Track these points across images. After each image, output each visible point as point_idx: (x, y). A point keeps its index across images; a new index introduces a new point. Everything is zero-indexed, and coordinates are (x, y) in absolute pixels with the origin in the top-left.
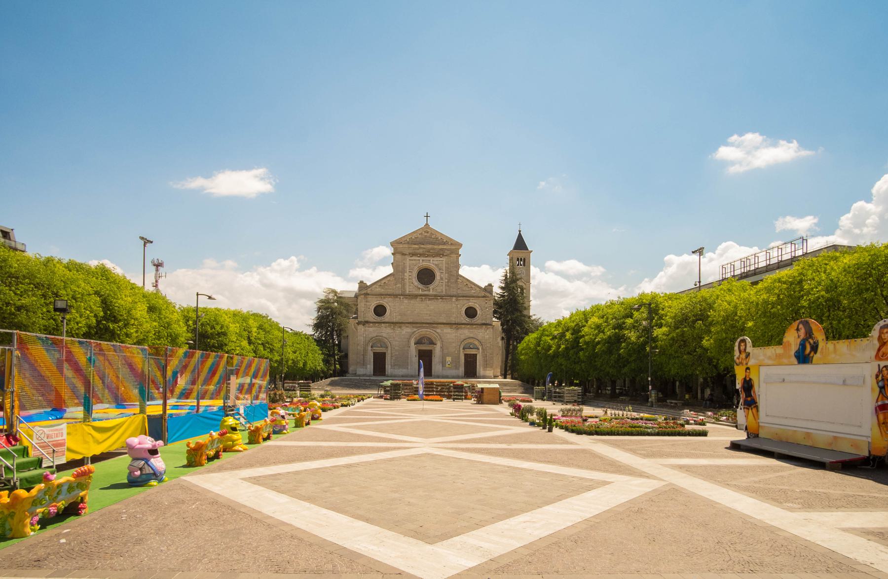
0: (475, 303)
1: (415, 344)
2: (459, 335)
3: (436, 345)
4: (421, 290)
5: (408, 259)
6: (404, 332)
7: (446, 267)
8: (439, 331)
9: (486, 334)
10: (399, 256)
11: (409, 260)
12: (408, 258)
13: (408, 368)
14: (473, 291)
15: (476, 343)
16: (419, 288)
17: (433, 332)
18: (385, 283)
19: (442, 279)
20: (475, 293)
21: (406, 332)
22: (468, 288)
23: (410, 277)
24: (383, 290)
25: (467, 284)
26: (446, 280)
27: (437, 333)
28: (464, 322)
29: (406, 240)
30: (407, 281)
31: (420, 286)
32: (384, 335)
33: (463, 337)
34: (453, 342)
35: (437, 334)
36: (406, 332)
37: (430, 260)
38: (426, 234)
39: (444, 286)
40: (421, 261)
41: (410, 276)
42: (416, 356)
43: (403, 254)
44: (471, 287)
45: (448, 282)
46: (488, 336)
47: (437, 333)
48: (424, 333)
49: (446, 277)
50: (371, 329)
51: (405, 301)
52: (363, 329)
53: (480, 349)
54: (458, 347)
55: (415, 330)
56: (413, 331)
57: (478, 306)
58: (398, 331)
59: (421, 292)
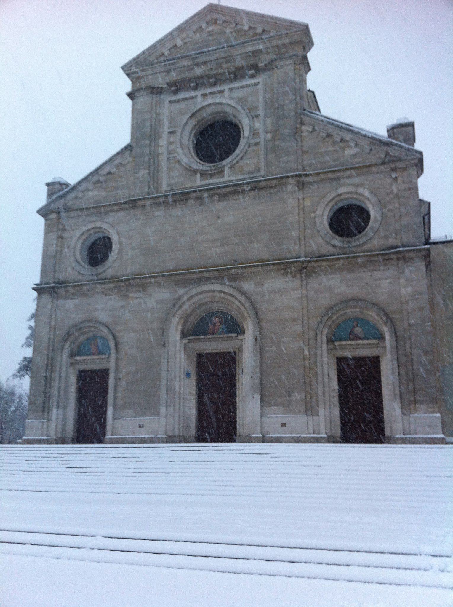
0: (357, 186)
1: (184, 335)
2: (312, 294)
3: (243, 333)
4: (198, 175)
5: (167, 102)
6: (151, 303)
7: (265, 100)
8: (248, 286)
9: (402, 281)
10: (144, 99)
11: (171, 102)
12: (167, 98)
13: (158, 414)
14: (349, 152)
15: (372, 315)
16: (195, 172)
17: (231, 291)
18: (109, 173)
19: (254, 133)
20: (354, 156)
21: (158, 302)
22: (335, 143)
23: (172, 147)
24: (103, 193)
25: (328, 136)
26: (269, 136)
27: (244, 293)
28: (327, 249)
29: (163, 54)
30: (163, 158)
31: (197, 164)
32: (103, 317)
33: (325, 300)
34: (294, 320)
35: (243, 299)
36: (158, 302)
37: (222, 92)
38: (210, 29)
39: (262, 152)
40: (199, 98)
41: (172, 143)
42: (188, 375)
43: (155, 91)
44: (342, 140)
45: (273, 139)
46: (409, 289)
47: (244, 293)
48: (205, 298)
49: (270, 127)
50: (70, 304)
51: (157, 214)
52: (49, 307)
53: (387, 336)
54: (312, 334)
55: (181, 291)
56: (177, 296)
57: (367, 193)
58: (136, 301)
59: (199, 181)
